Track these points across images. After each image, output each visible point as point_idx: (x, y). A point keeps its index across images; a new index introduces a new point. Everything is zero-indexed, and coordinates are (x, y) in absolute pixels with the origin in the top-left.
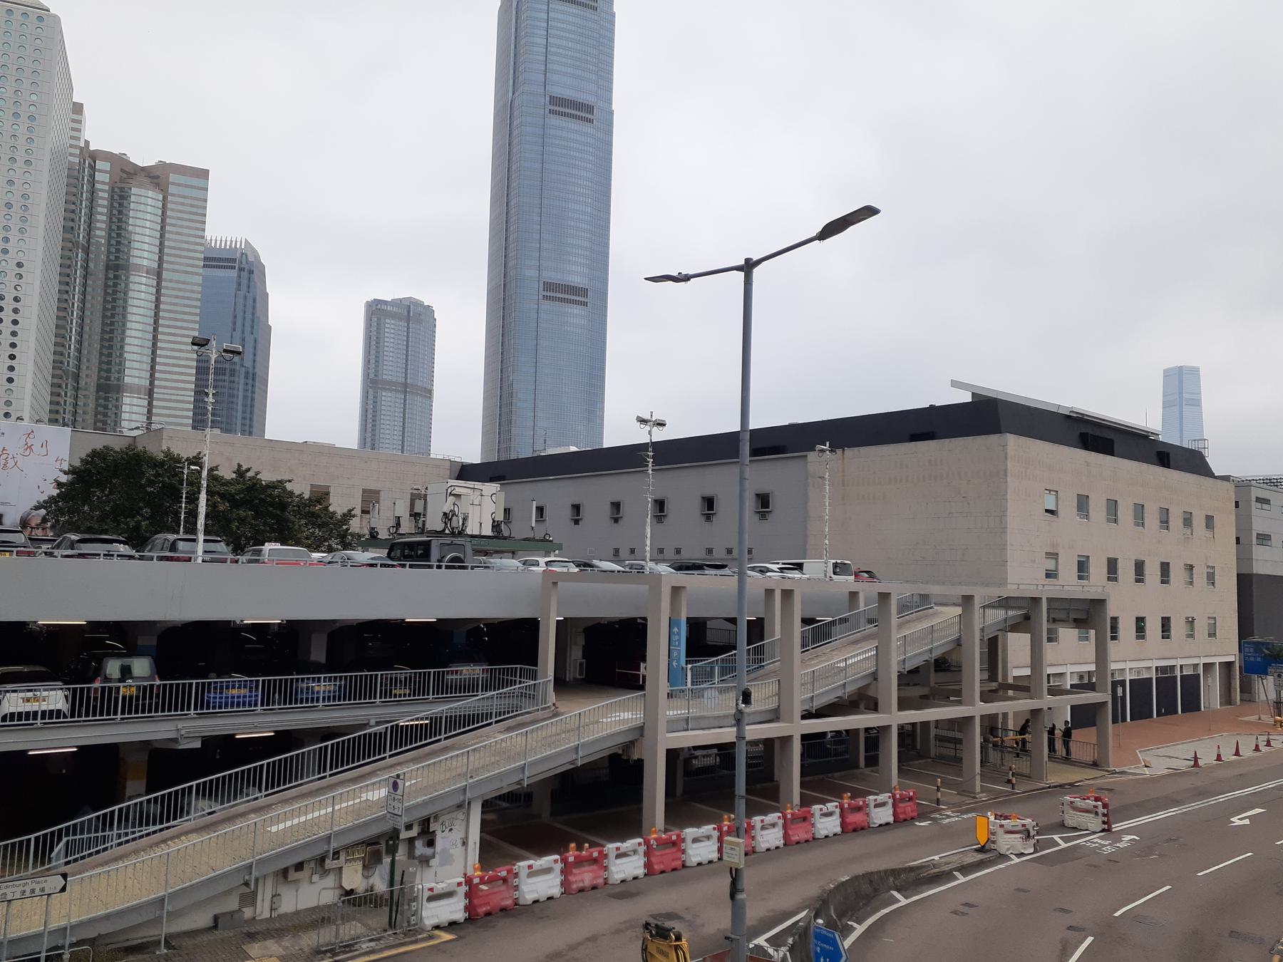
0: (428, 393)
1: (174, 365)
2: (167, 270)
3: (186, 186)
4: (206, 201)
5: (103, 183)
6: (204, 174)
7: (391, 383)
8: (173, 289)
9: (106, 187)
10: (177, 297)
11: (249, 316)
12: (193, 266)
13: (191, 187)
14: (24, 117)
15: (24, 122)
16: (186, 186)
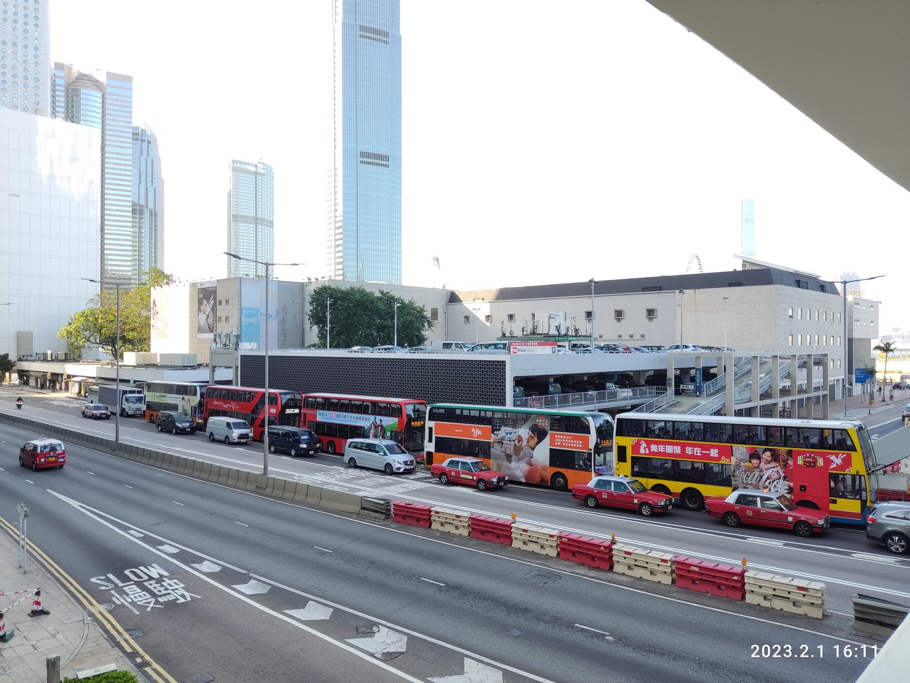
0: (271, 224)
1: (117, 210)
2: (109, 145)
3: (118, 87)
4: (131, 97)
5: (61, 85)
6: (128, 79)
7: (246, 217)
8: (113, 158)
9: (63, 89)
10: (117, 164)
11: (149, 174)
12: (126, 142)
13: (121, 88)
14: (31, 48)
15: (31, 52)
16: (118, 87)
